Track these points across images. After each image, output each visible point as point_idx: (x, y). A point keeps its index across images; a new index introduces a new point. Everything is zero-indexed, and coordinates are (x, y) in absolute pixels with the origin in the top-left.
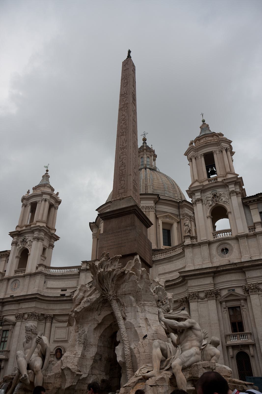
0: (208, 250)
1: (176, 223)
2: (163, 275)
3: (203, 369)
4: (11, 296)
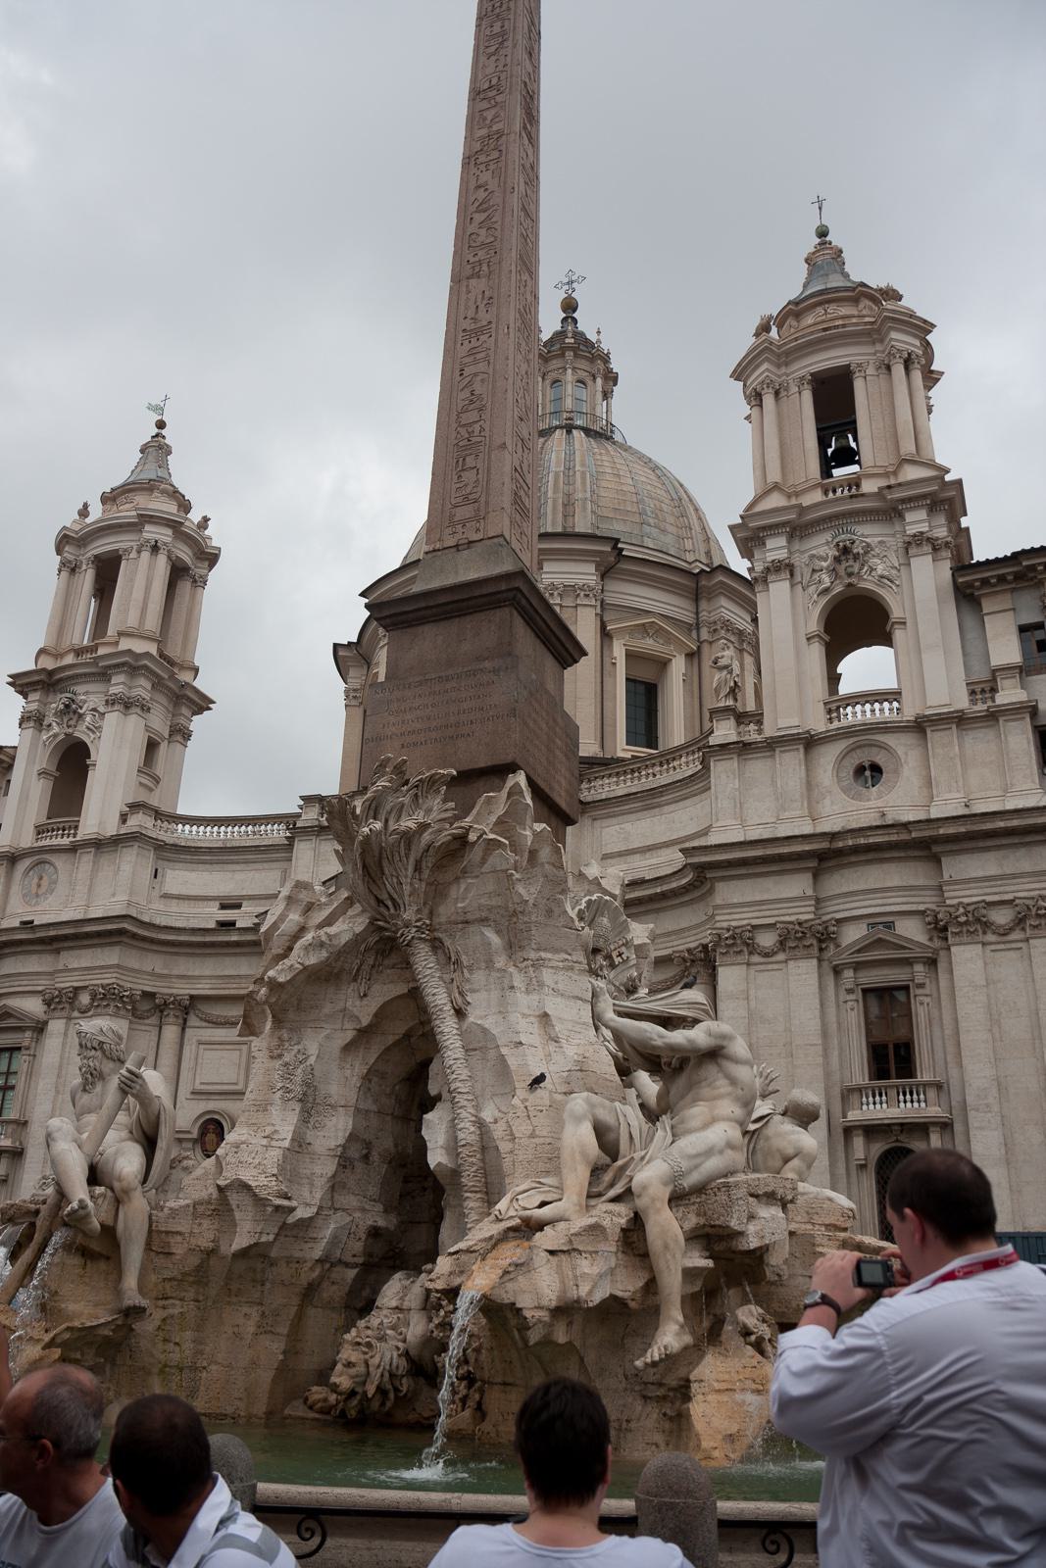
1: (683, 655)
2: (623, 859)
3: (751, 1199)
4: (23, 923)
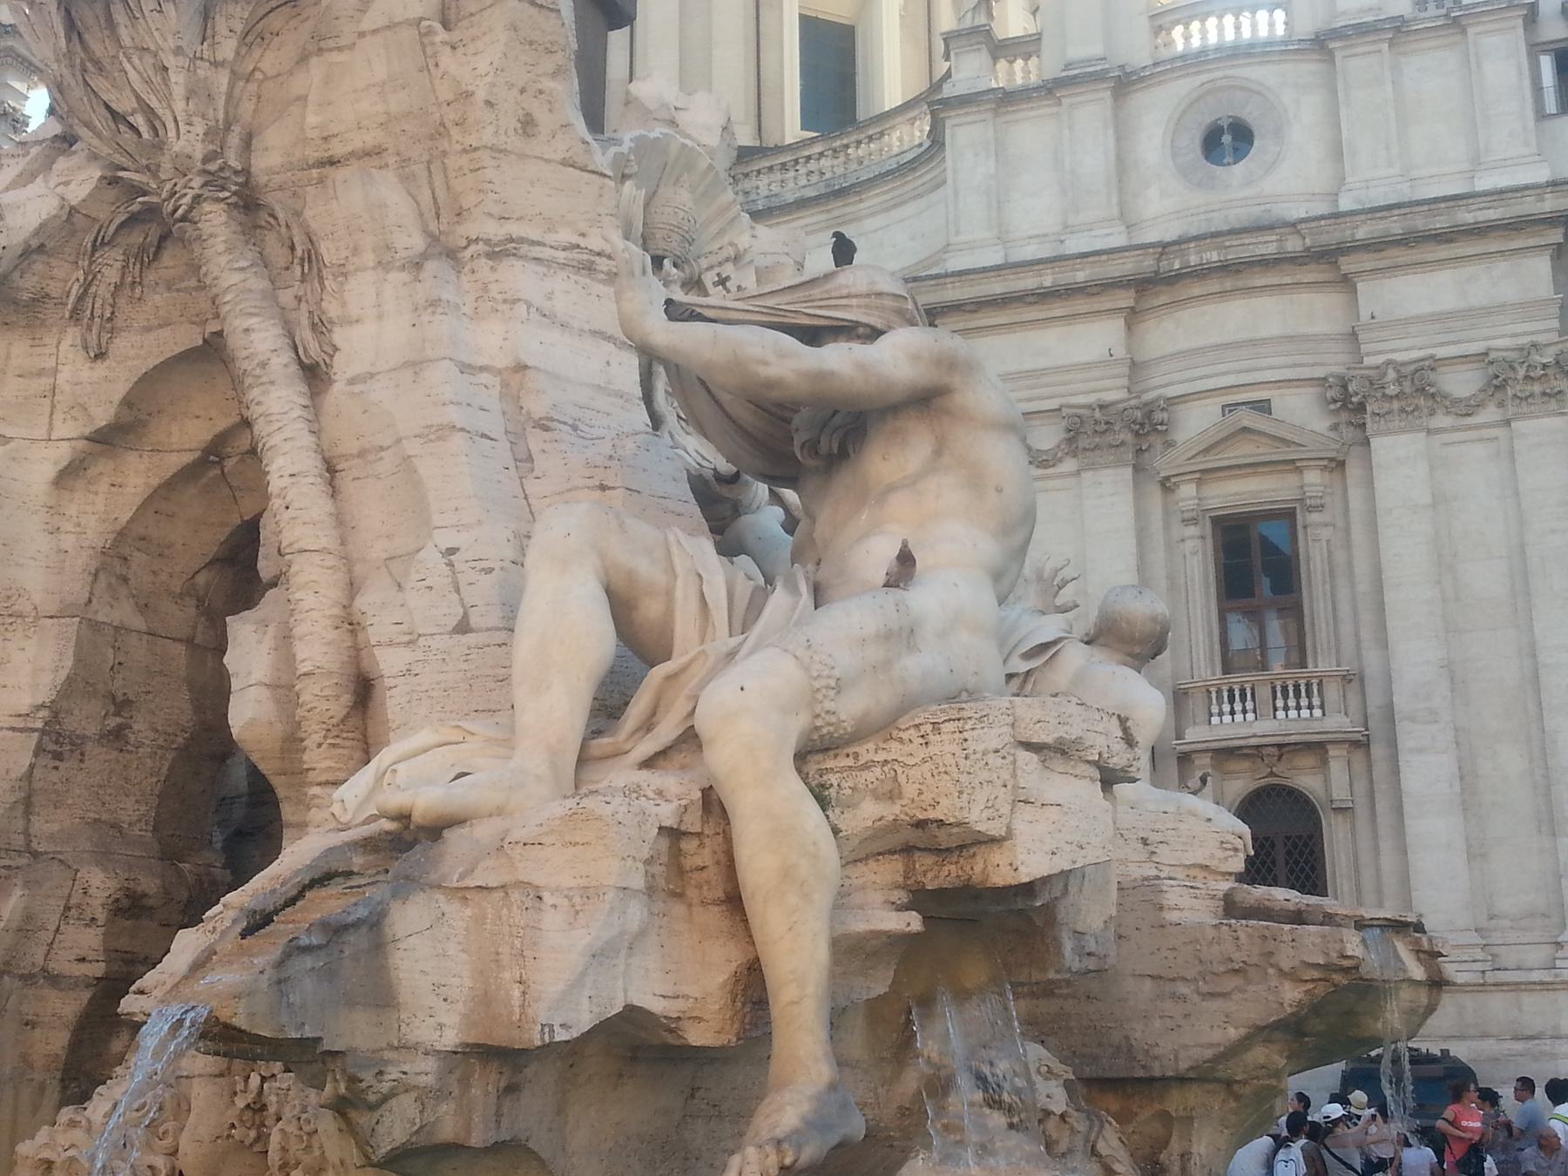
0: (1111, 132)
